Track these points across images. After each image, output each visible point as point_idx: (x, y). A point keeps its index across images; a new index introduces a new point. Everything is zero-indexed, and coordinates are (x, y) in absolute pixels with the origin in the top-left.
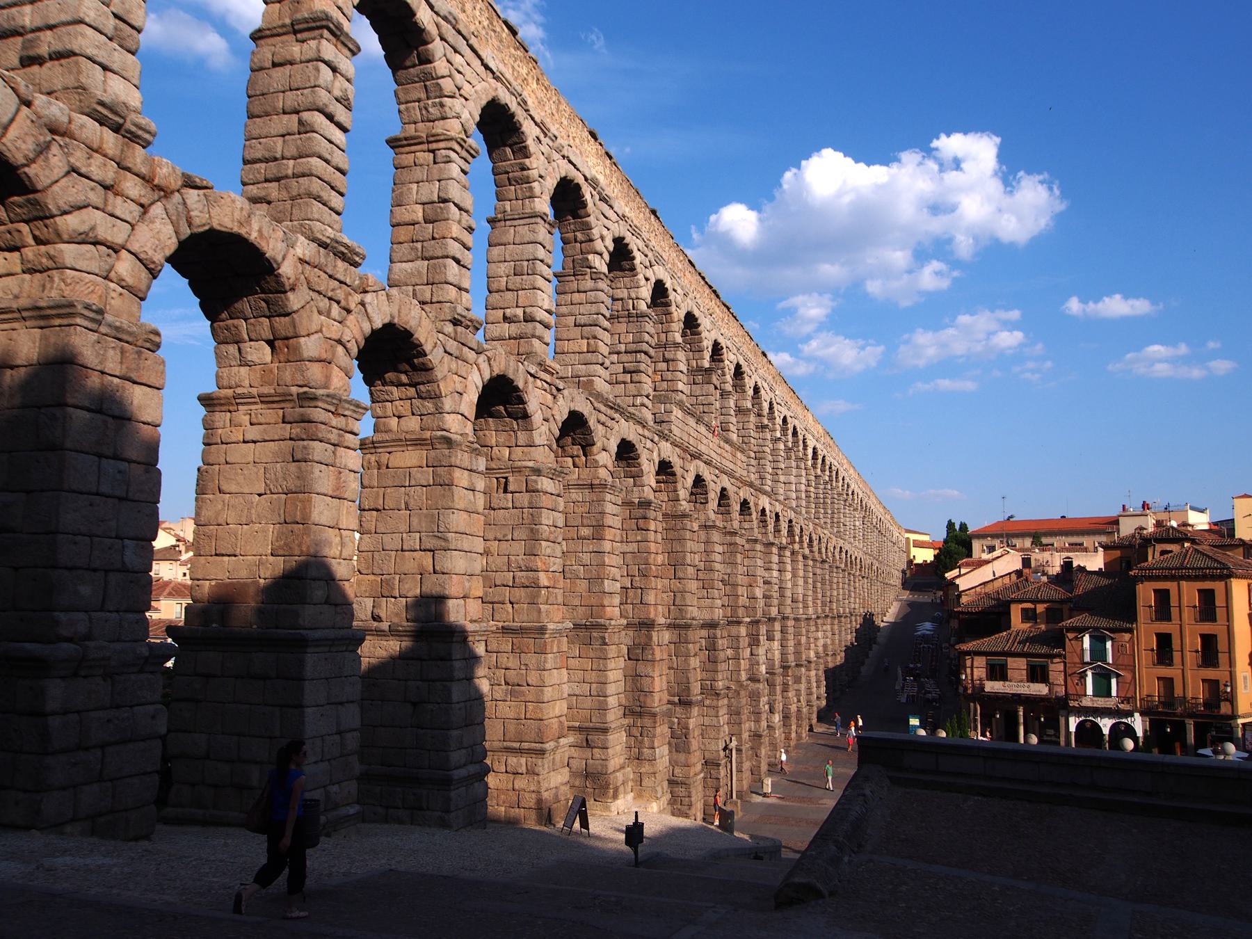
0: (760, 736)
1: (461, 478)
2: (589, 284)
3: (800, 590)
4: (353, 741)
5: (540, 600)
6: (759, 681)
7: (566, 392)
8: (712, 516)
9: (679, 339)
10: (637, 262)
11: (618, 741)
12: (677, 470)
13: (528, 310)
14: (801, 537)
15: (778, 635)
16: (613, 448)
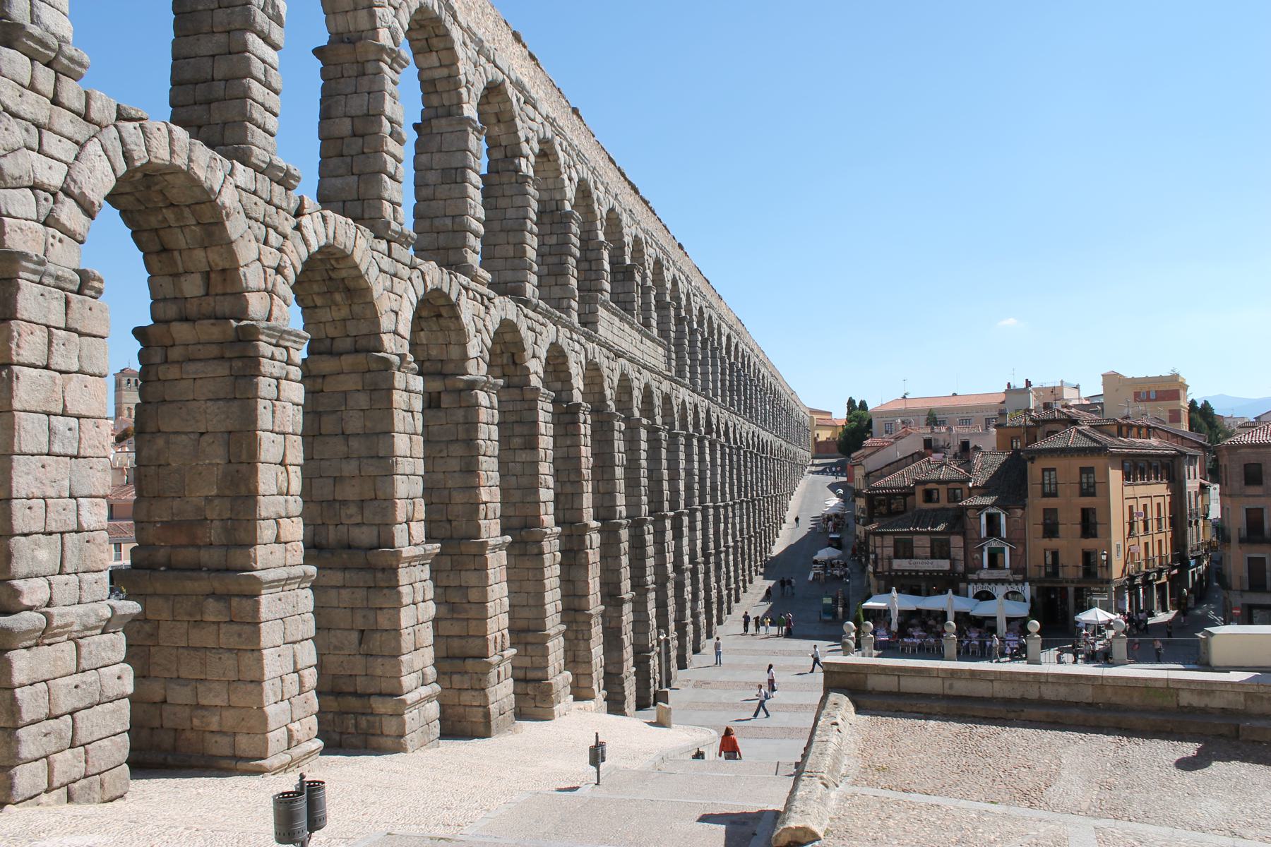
1: (399, 398)
4: (311, 677)
5: (482, 514)
8: (637, 414)
9: (602, 237)
10: (562, 161)
11: (556, 649)
12: (606, 372)
15: (699, 525)
16: (543, 354)
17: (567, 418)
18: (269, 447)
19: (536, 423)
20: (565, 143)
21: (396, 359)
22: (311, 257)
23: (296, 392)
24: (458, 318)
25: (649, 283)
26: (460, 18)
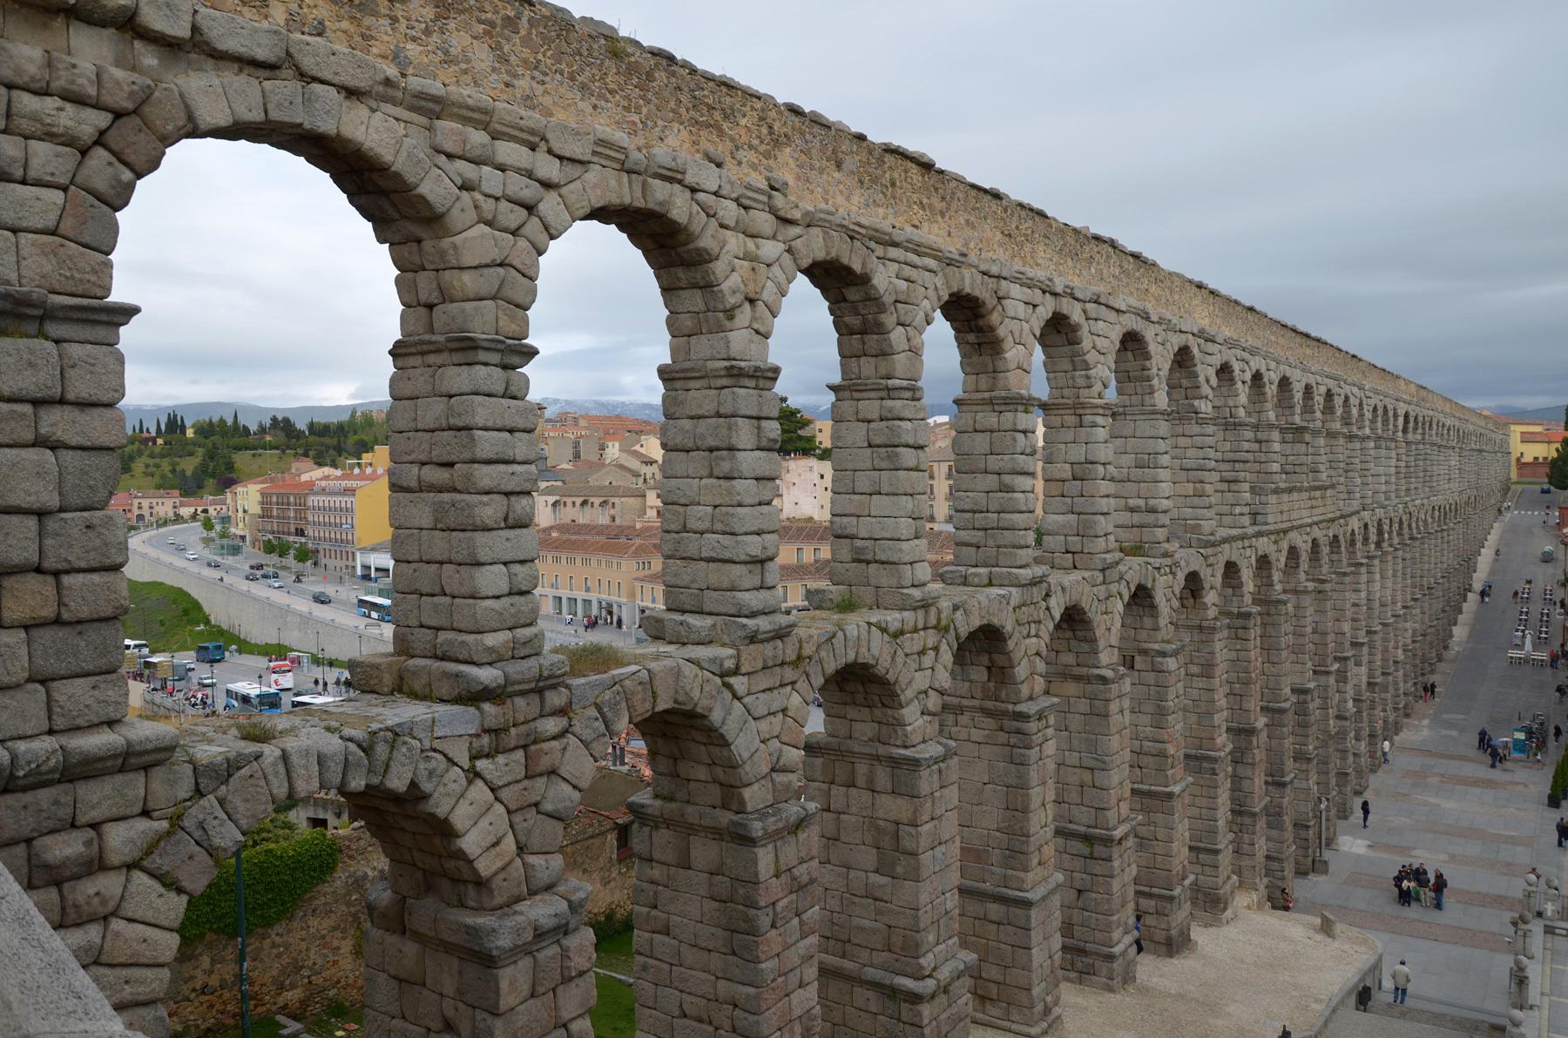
0: (1346, 774)
1: (1114, 707)
2: (1196, 429)
3: (1389, 592)
4: (1058, 957)
6: (1346, 719)
7: (1183, 563)
8: (1302, 576)
9: (1272, 415)
10: (1237, 372)
11: (1225, 859)
12: (1273, 558)
13: (1151, 502)
14: (1390, 533)
15: (1365, 659)
16: (1219, 579)
17: (1240, 622)
18: (1036, 794)
19: (1212, 653)
20: (1239, 352)
21: (1109, 673)
22: (1058, 627)
23: (1050, 748)
24: (1151, 597)
25: (1319, 424)
26: (1154, 318)
